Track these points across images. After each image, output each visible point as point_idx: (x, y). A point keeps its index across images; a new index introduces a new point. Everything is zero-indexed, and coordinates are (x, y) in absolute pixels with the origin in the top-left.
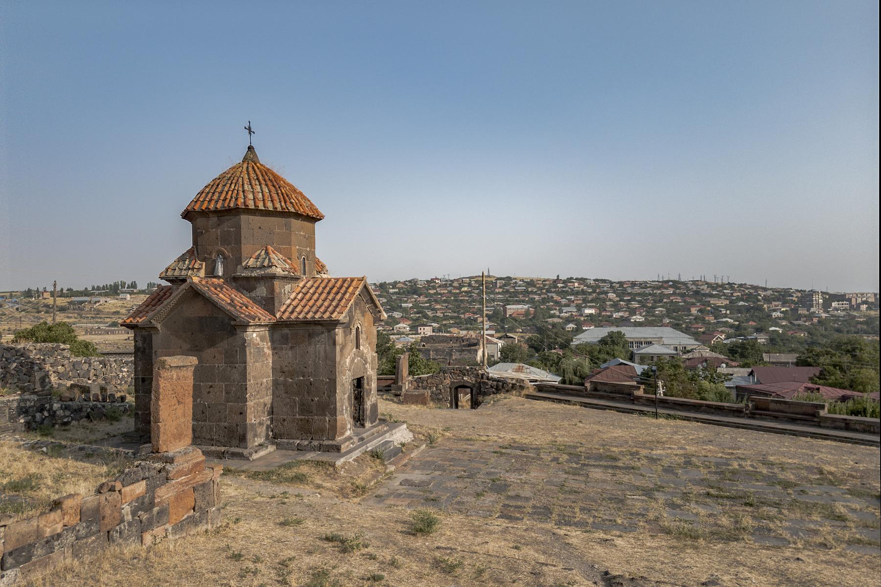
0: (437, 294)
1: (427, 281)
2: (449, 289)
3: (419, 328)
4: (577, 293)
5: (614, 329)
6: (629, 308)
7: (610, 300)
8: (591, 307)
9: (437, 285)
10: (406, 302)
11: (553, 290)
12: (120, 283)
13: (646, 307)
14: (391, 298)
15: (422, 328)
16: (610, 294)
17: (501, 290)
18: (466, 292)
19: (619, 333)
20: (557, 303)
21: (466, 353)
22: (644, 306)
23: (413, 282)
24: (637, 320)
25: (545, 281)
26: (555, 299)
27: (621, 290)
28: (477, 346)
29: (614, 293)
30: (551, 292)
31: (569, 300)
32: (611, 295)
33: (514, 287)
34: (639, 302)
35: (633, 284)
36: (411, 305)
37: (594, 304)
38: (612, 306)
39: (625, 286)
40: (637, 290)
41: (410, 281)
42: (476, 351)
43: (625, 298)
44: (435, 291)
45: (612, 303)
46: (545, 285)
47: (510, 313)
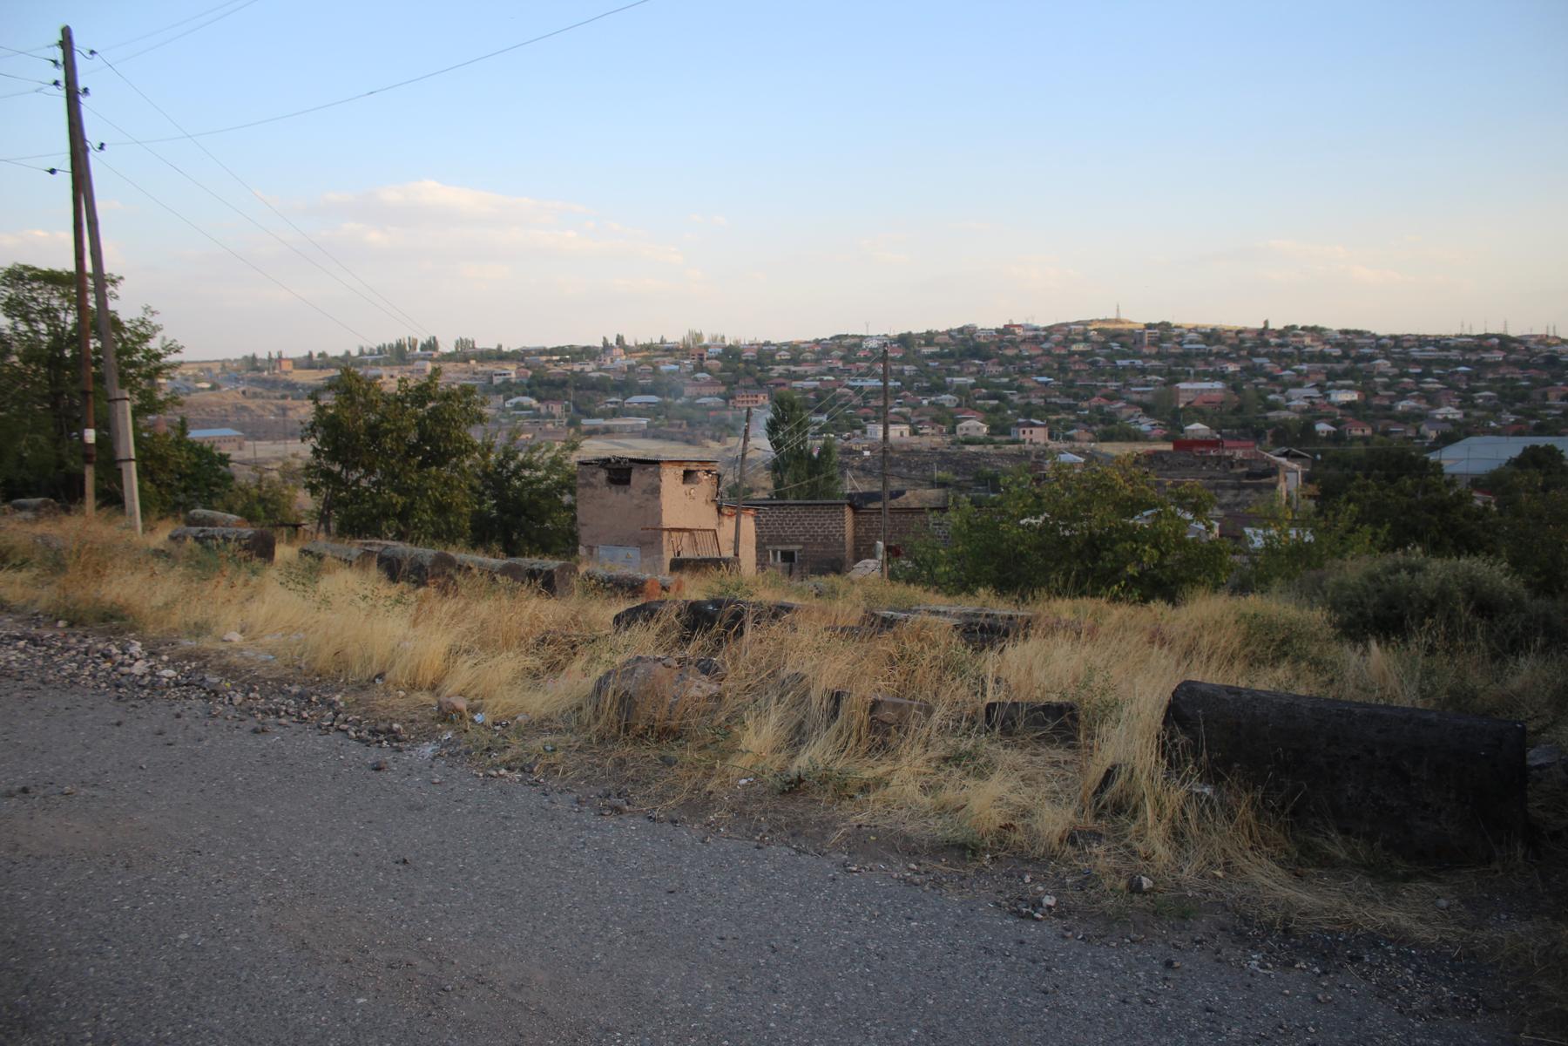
0: (1019, 357)
1: (997, 330)
2: (1046, 346)
3: (1021, 430)
4: (1312, 358)
5: (1542, 441)
6: (1421, 390)
7: (1381, 374)
8: (1349, 388)
9: (1019, 339)
10: (959, 373)
11: (1263, 351)
12: (407, 341)
13: (1458, 389)
14: (927, 365)
15: (1028, 430)
16: (1378, 362)
17: (1154, 350)
18: (1082, 354)
19: (1550, 451)
20: (1273, 378)
21: (1248, 491)
22: (1450, 387)
23: (966, 333)
24: (1450, 417)
25: (1239, 332)
26: (1269, 370)
27: (1400, 353)
28: (1274, 478)
29: (1387, 358)
30: (1258, 356)
31: (1299, 373)
32: (1382, 364)
33: (1180, 344)
34: (1439, 377)
35: (1422, 341)
36: (972, 381)
37: (1350, 382)
39: (1406, 344)
40: (1431, 353)
41: (961, 330)
42: (1273, 486)
43: (1411, 370)
45: (1386, 380)
46: (1242, 341)
47: (1186, 400)
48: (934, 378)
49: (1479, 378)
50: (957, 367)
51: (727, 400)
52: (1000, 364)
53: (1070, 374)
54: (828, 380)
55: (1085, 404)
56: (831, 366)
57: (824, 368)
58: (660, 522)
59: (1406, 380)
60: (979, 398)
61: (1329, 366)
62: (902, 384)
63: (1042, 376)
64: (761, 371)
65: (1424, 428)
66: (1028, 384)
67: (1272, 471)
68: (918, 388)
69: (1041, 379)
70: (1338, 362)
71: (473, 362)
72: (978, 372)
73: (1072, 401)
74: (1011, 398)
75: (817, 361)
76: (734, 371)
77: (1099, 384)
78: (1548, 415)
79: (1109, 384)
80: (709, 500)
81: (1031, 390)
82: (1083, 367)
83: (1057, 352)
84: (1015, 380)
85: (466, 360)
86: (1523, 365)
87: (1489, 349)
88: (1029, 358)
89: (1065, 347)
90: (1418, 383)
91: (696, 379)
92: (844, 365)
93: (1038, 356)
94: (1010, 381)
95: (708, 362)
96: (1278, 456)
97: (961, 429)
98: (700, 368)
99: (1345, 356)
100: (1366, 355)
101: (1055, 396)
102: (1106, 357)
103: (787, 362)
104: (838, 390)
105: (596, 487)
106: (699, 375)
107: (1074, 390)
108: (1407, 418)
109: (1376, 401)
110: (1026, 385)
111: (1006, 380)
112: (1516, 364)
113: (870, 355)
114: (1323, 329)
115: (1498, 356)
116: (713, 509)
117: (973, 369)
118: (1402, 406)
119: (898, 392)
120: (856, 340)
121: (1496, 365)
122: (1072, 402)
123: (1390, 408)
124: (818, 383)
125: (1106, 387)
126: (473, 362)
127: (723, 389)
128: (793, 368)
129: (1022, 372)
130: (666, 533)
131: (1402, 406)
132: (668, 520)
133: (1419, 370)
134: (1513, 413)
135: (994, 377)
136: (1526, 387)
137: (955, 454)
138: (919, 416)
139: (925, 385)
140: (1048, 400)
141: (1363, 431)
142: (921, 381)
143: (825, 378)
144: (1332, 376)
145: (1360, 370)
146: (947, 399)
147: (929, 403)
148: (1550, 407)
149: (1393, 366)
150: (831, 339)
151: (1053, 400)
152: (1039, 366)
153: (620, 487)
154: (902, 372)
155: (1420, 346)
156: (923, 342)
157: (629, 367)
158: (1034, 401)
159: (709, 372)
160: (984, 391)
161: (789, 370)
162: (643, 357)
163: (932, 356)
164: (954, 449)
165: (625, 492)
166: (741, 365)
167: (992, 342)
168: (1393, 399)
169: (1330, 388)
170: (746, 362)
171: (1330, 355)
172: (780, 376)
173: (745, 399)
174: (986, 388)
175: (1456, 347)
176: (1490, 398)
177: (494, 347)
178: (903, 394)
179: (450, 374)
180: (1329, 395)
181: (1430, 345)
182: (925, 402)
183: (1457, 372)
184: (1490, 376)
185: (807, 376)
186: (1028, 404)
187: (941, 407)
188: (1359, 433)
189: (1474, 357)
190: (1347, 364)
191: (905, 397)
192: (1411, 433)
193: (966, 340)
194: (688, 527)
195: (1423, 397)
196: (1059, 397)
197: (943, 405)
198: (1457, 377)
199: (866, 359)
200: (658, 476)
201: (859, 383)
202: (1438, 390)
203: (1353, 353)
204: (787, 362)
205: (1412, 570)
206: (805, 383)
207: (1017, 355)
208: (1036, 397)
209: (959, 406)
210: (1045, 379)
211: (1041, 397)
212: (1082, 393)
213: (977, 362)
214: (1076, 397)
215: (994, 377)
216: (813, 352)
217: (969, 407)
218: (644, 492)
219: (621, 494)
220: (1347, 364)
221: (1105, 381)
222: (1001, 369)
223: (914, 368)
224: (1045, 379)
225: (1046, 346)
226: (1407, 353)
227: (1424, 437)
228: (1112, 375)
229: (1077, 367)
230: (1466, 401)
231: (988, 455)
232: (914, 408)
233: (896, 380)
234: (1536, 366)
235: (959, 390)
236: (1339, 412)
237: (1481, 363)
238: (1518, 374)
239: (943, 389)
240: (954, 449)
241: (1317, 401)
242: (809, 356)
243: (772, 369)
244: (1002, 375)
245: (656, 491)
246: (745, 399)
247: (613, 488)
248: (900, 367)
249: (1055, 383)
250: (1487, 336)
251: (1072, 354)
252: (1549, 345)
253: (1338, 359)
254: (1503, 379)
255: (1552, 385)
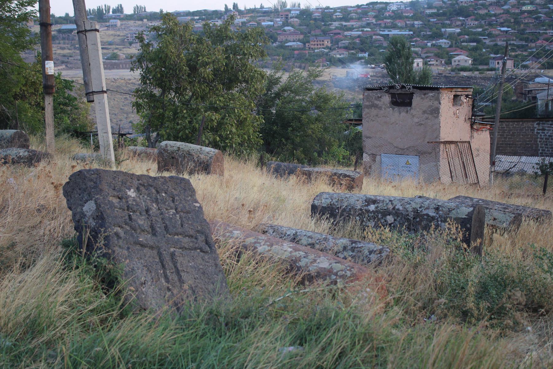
0: (489, 15)
2: (505, 7)
3: (497, 62)
9: (487, 4)
10: (450, 26)
12: (104, 7)
14: (429, 21)
18: (529, 12)
36: (458, 30)
44: (486, 11)
48: (434, 29)
50: (448, 22)
51: (304, 44)
52: (476, 20)
53: (522, 26)
54: (367, 31)
55: (533, 45)
56: (368, 22)
57: (364, 23)
58: (438, 136)
60: (463, 42)
62: (414, 33)
63: (503, 27)
64: (324, 25)
66: (495, 32)
68: (424, 36)
69: (503, 29)
71: (145, 20)
72: (462, 25)
73: (524, 43)
74: (484, 41)
75: (359, 19)
76: (308, 26)
77: (541, 32)
79: (548, 31)
80: (467, 119)
81: (497, 36)
82: (530, 21)
83: (513, 11)
84: (487, 29)
85: (141, 20)
88: (495, 15)
89: (518, 8)
91: (285, 31)
92: (376, 21)
93: (500, 14)
94: (482, 30)
95: (292, 20)
97: (455, 61)
98: (286, 24)
101: (513, 40)
102: (545, 14)
103: (341, 19)
104: (374, 37)
105: (380, 108)
106: (286, 28)
107: (526, 36)
110: (494, 33)
111: (480, 30)
113: (392, 15)
116: (468, 126)
117: (459, 23)
119: (411, 38)
120: (384, 6)
122: (524, 43)
124: (361, 33)
125: (546, 33)
126: (145, 20)
127: (301, 37)
128: (344, 23)
129: (490, 24)
130: (442, 146)
132: (445, 135)
135: (472, 28)
137: (454, 77)
138: (426, 53)
139: (428, 33)
140: (509, 42)
142: (426, 31)
143: (365, 29)
146: (443, 42)
147: (432, 45)
150: (367, 5)
151: (512, 42)
152: (502, 20)
153: (402, 108)
154: (413, 25)
156: (426, 6)
157: (242, 23)
158: (499, 43)
159: (292, 26)
160: (466, 37)
161: (342, 25)
162: (251, 17)
163: (432, 15)
164: (453, 74)
165: (407, 112)
166: (312, 22)
167: (470, 6)
170: (315, 20)
172: (337, 28)
173: (316, 43)
174: (468, 35)
177: (158, 11)
178: (414, 39)
179: (132, 28)
182: (429, 44)
185: (354, 29)
186: (496, 45)
187: (440, 47)
191: (416, 41)
193: (454, 5)
194: (454, 140)
196: (515, 40)
197: (440, 46)
199: (390, 17)
200: (438, 100)
201: (386, 32)
204: (341, 19)
206: (353, 33)
207: (487, 14)
208: (500, 40)
209: (451, 46)
210: (505, 29)
211: (504, 41)
212: (531, 38)
213: (461, 18)
214: (527, 40)
215: (472, 28)
216: (356, 13)
217: (458, 47)
218: (424, 112)
219: (403, 114)
221: (546, 30)
222: (476, 23)
223: (421, 23)
224: (505, 29)
225: (505, 7)
228: (550, 26)
229: (526, 21)
231: (476, 78)
232: (422, 48)
233: (410, 31)
235: (450, 37)
239: (440, 36)
240: (453, 74)
242: (354, 15)
243: (331, 24)
244: (477, 27)
245: (435, 112)
246: (316, 43)
247: (396, 109)
248: (412, 22)
249: (513, 31)
251: (523, 12)
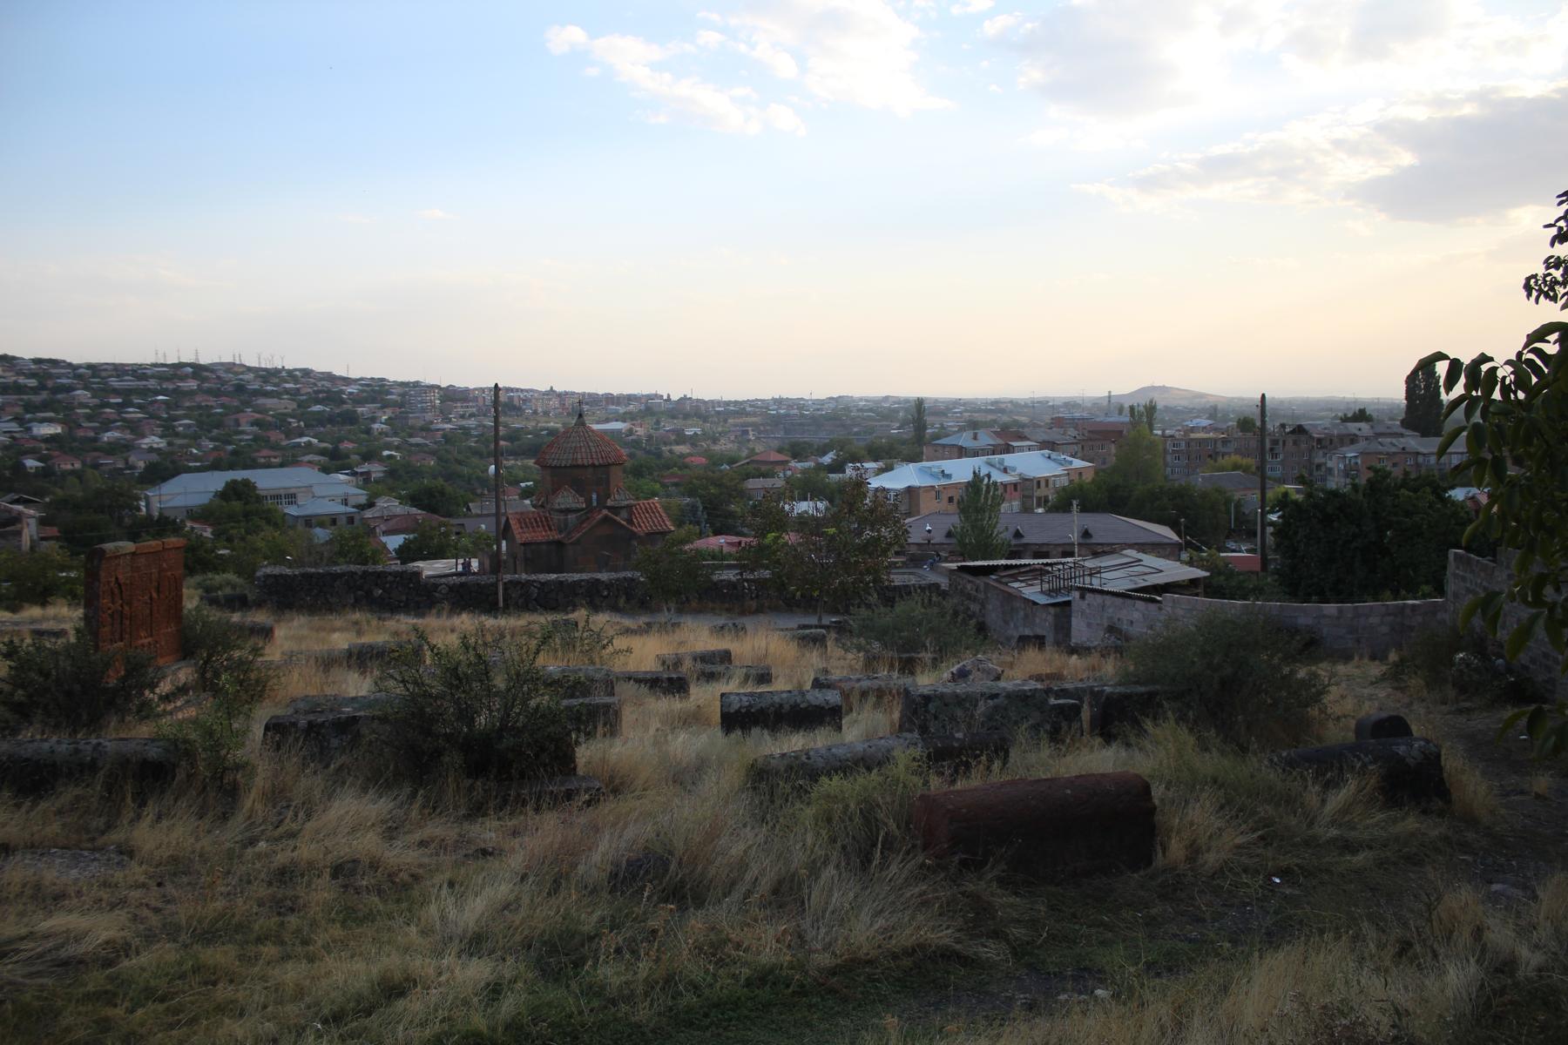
5: (239, 475)
6: (124, 420)
8: (50, 421)
13: (159, 418)
16: (79, 392)
19: (246, 483)
22: (152, 416)
24: (155, 446)
27: (98, 383)
28: (18, 526)
29: (86, 388)
32: (82, 394)
34: (140, 407)
35: (119, 370)
37: (52, 414)
38: (89, 418)
39: (104, 374)
40: (129, 382)
42: (19, 533)
43: (112, 401)
45: (88, 411)
49: (177, 407)
59: (108, 410)
61: (25, 397)
65: (132, 459)
67: (17, 519)
70: (36, 394)
78: (241, 440)
86: (216, 393)
87: (183, 378)
90: (120, 413)
96: (11, 503)
99: (42, 387)
100: (63, 385)
108: (114, 449)
109: (80, 433)
112: (209, 392)
114: (14, 358)
115: (192, 384)
118: (107, 436)
121: (191, 393)
123: (95, 440)
131: (107, 436)
133: (120, 400)
134: (212, 439)
136: (219, 414)
141: (73, 465)
144: (29, 407)
145: (59, 401)
148: (243, 432)
149: (93, 397)
155: (118, 376)
168: (97, 431)
169: (31, 421)
171: (26, 386)
175: (153, 377)
176: (188, 426)
180: (29, 429)
181: (128, 375)
183: (156, 401)
184: (187, 404)
188: (69, 467)
189: (171, 386)
190: (44, 395)
192: (120, 465)
195: (128, 427)
198: (156, 405)
202: (140, 420)
203: (50, 383)
205: (211, 579)
220: (44, 395)
226: (106, 383)
227: (133, 467)
230: (168, 430)
234: (226, 394)
236: (43, 445)
237: (177, 392)
238: (211, 401)
241: (17, 435)
250: (181, 365)
252: (237, 373)
253: (35, 390)
254: (199, 407)
255: (243, 411)
